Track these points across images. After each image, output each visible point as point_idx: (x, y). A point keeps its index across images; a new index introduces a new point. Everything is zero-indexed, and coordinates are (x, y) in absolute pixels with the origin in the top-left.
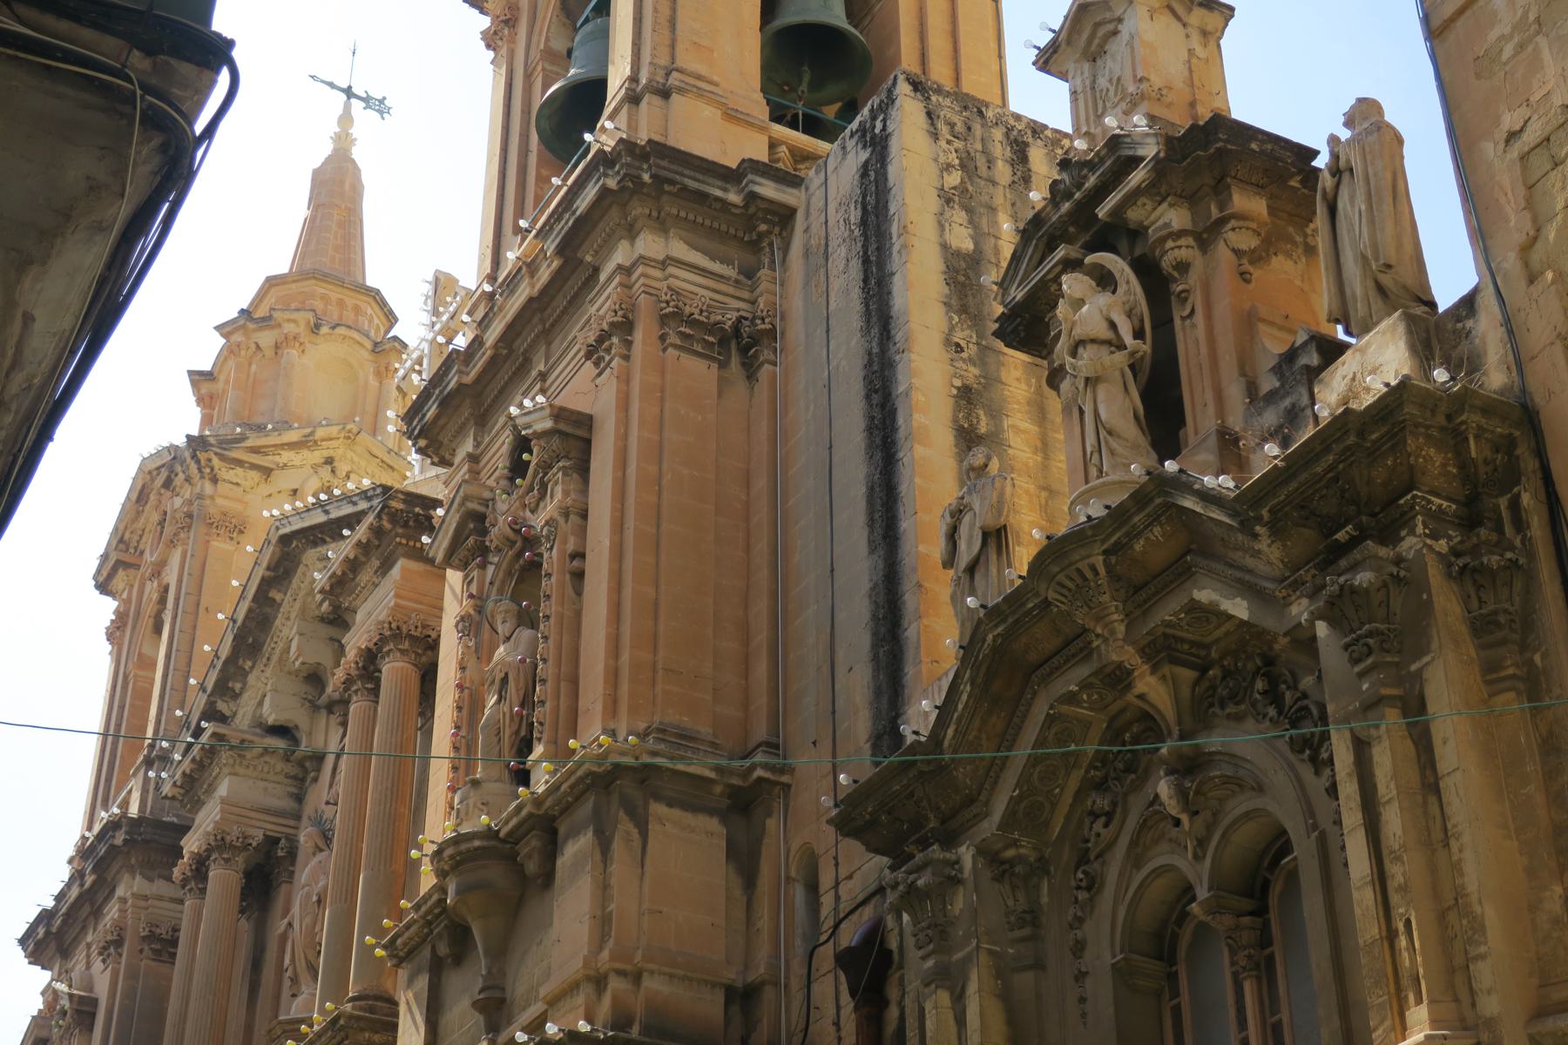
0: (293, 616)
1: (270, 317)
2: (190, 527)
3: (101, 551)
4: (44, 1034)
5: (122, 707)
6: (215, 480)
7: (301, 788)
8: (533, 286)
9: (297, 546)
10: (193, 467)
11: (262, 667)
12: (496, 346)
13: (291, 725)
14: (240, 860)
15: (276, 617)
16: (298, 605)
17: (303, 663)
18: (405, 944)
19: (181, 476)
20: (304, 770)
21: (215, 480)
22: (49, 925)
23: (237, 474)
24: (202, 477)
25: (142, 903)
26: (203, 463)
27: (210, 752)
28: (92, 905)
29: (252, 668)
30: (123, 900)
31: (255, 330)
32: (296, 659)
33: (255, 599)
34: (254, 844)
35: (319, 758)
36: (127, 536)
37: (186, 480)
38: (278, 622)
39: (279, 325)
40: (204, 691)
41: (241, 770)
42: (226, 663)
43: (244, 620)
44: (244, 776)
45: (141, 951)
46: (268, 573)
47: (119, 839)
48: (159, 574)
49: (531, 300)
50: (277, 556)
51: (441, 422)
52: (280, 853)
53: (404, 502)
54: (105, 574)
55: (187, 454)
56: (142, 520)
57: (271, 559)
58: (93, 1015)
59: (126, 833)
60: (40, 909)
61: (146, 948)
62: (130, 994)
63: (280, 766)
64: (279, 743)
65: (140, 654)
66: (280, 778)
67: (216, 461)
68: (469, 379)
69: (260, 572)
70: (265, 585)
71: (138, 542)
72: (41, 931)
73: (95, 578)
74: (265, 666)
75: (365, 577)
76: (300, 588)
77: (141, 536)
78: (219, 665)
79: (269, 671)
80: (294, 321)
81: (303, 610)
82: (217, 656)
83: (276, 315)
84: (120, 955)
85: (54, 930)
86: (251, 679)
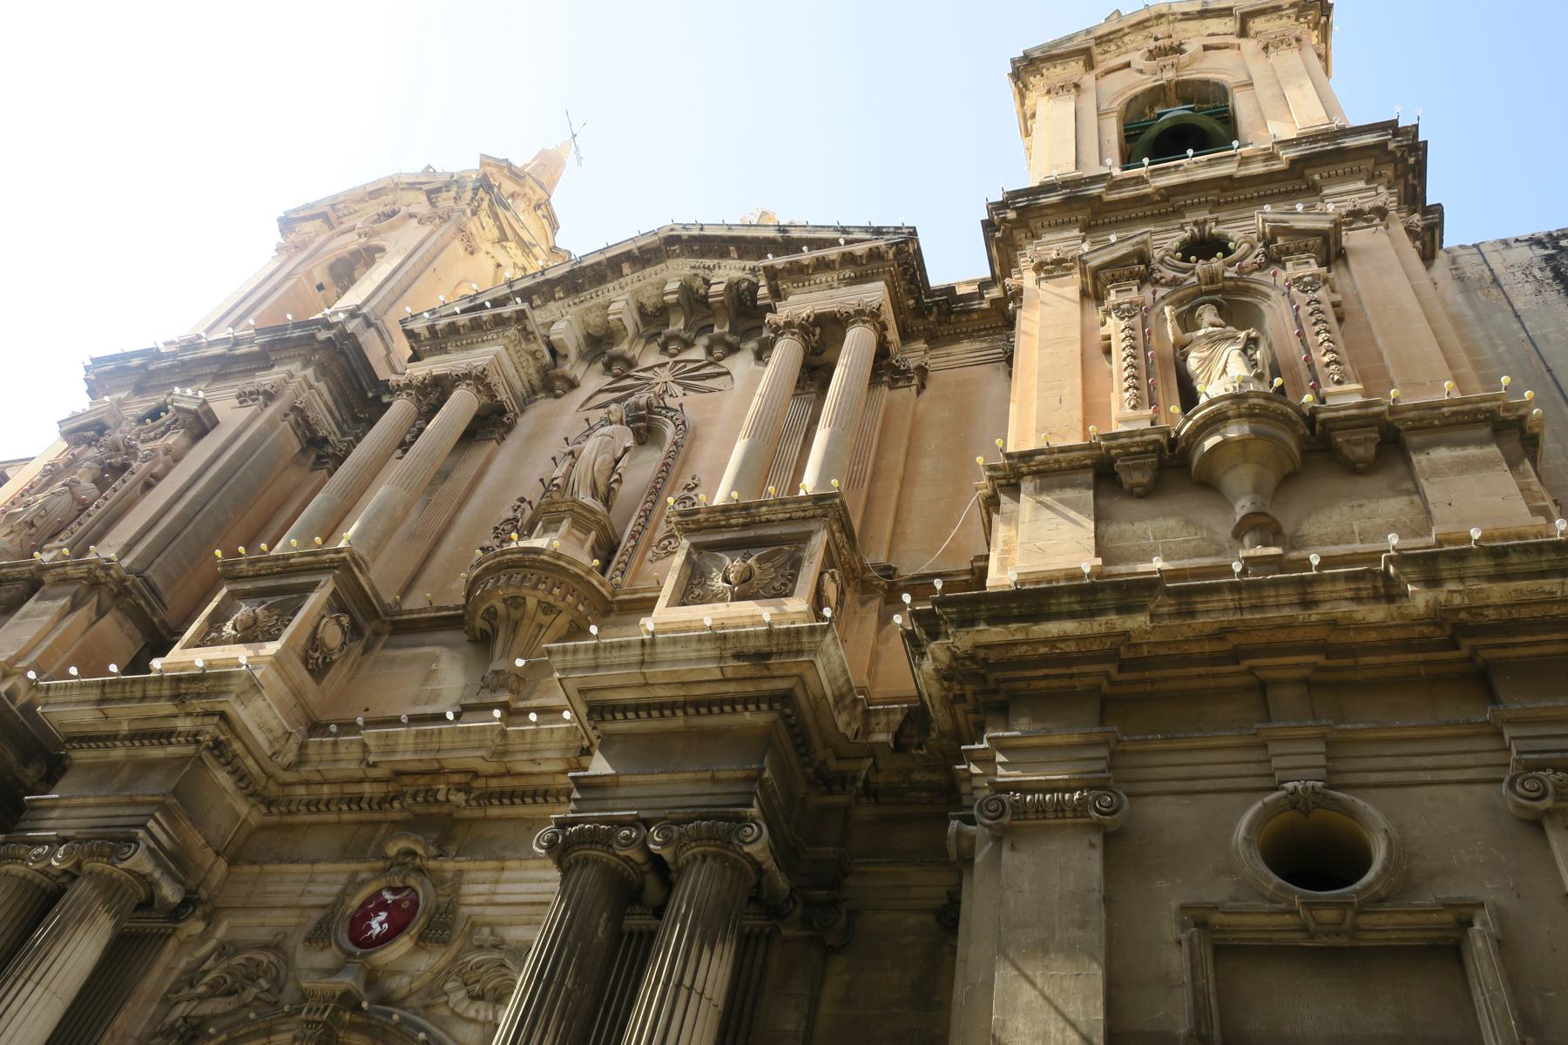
0: (627, 289)
1: (522, 178)
2: (445, 221)
3: (310, 201)
4: (110, 422)
5: (275, 288)
6: (474, 213)
7: (529, 397)
8: (1238, 171)
9: (675, 250)
10: (468, 195)
11: (571, 303)
12: (1158, 190)
13: (562, 352)
14: (485, 399)
15: (611, 281)
16: (638, 285)
17: (620, 320)
18: (1042, 463)
19: (452, 194)
20: (552, 383)
21: (474, 213)
22: (151, 361)
23: (489, 222)
24: (469, 205)
25: (305, 387)
26: (477, 197)
27: (500, 322)
28: (220, 369)
29: (560, 299)
30: (291, 376)
31: (505, 176)
32: (614, 314)
33: (609, 259)
34: (499, 398)
35: (572, 385)
36: (339, 207)
37: (455, 198)
38: (610, 286)
39: (523, 186)
40: (510, 287)
41: (512, 350)
42: (547, 281)
43: (587, 267)
44: (510, 355)
45: (286, 415)
46: (636, 251)
47: (323, 335)
48: (370, 237)
49: (1230, 178)
50: (654, 245)
51: (1049, 211)
52: (505, 419)
53: (914, 251)
54: (302, 214)
55: (470, 186)
56: (362, 206)
57: (648, 244)
58: (204, 432)
59: (335, 335)
60: (153, 346)
61: (292, 417)
62: (262, 435)
63: (532, 371)
64: (548, 358)
65: (310, 270)
66: (525, 378)
67: (485, 204)
68: (1107, 198)
69: (632, 246)
70: (628, 257)
71: (345, 215)
72: (135, 362)
73: (287, 213)
74: (575, 304)
75: (821, 277)
76: (650, 276)
77: (350, 214)
78: (540, 279)
79: (574, 309)
80: (534, 191)
81: (636, 292)
82: (543, 273)
83: (528, 178)
84: (266, 406)
85: (151, 368)
86: (552, 305)
